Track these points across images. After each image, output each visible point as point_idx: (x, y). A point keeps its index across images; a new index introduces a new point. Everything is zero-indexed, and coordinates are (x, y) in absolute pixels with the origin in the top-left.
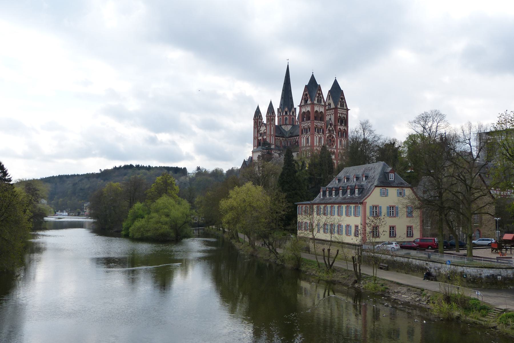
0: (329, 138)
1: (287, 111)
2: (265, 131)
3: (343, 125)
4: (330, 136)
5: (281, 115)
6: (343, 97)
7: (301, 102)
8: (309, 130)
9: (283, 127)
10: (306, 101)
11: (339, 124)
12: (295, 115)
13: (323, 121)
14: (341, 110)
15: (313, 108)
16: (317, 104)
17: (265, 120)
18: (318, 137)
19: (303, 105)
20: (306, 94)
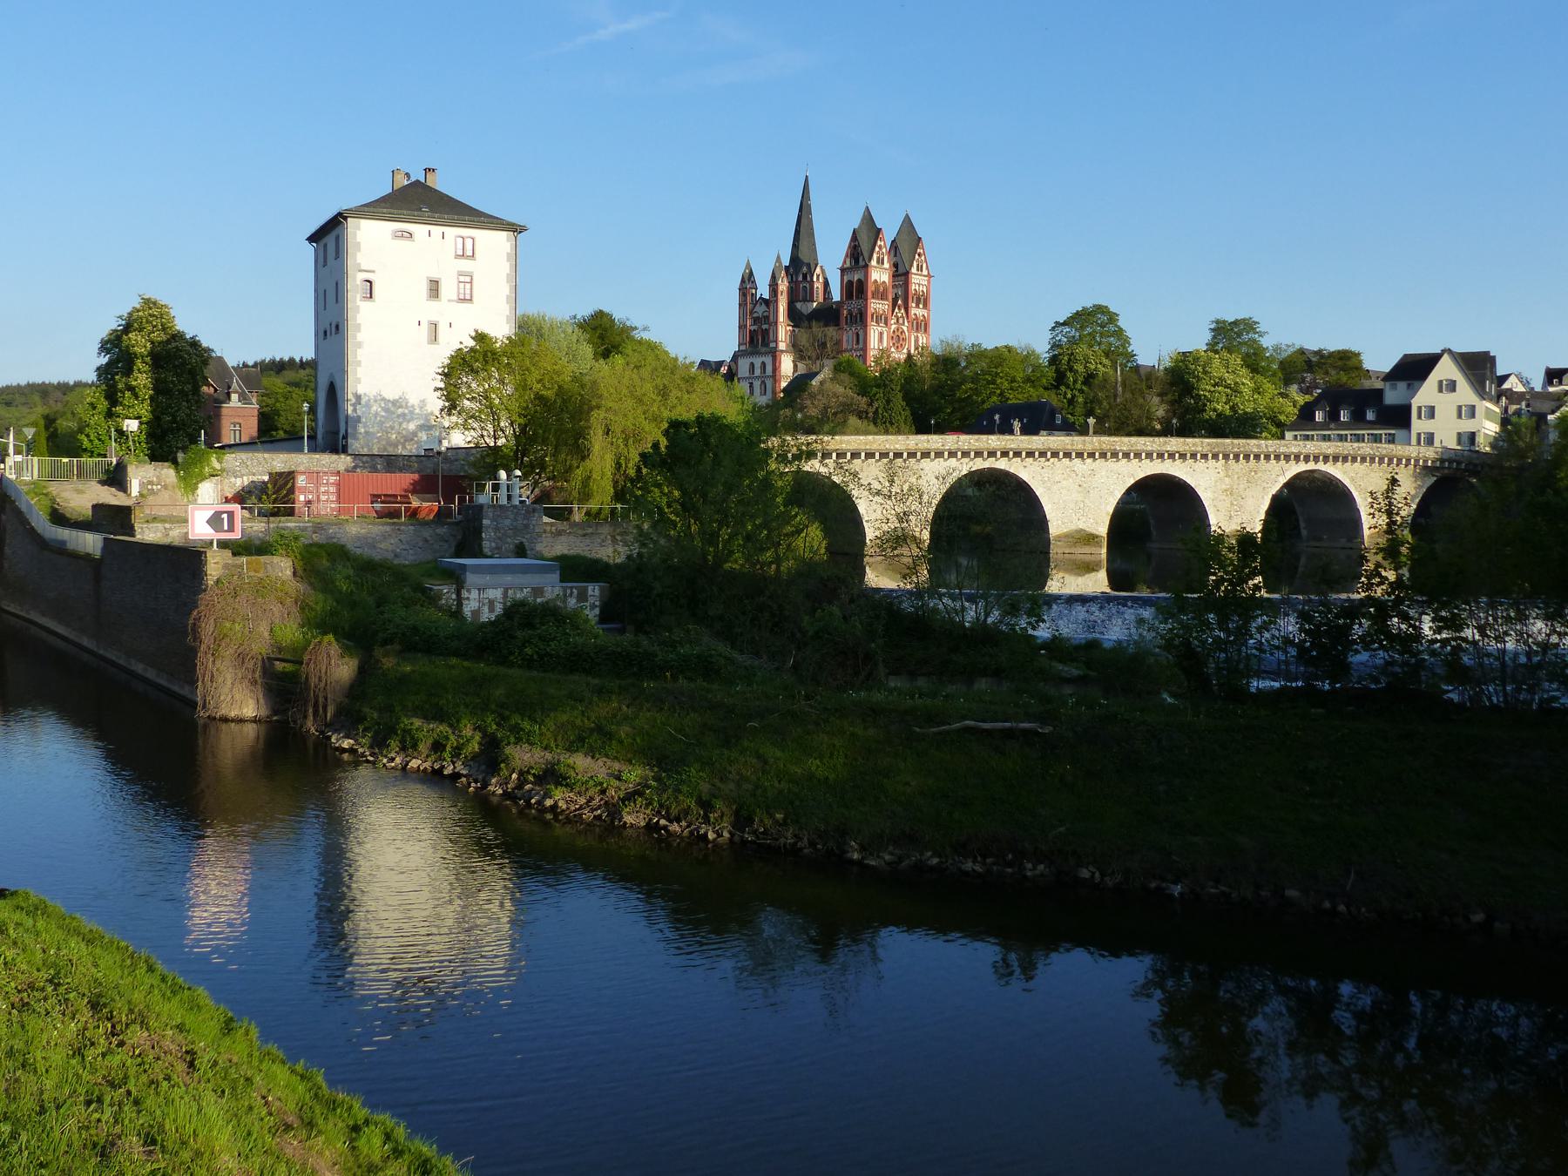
0: (896, 334)
1: (806, 274)
2: (765, 314)
3: (921, 306)
4: (898, 330)
5: (794, 279)
6: (922, 251)
7: (845, 262)
8: (861, 317)
9: (799, 305)
10: (857, 261)
11: (914, 305)
12: (821, 280)
13: (887, 299)
14: (918, 277)
15: (867, 275)
16: (875, 267)
17: (763, 291)
18: (876, 331)
19: (848, 268)
20: (855, 245)
